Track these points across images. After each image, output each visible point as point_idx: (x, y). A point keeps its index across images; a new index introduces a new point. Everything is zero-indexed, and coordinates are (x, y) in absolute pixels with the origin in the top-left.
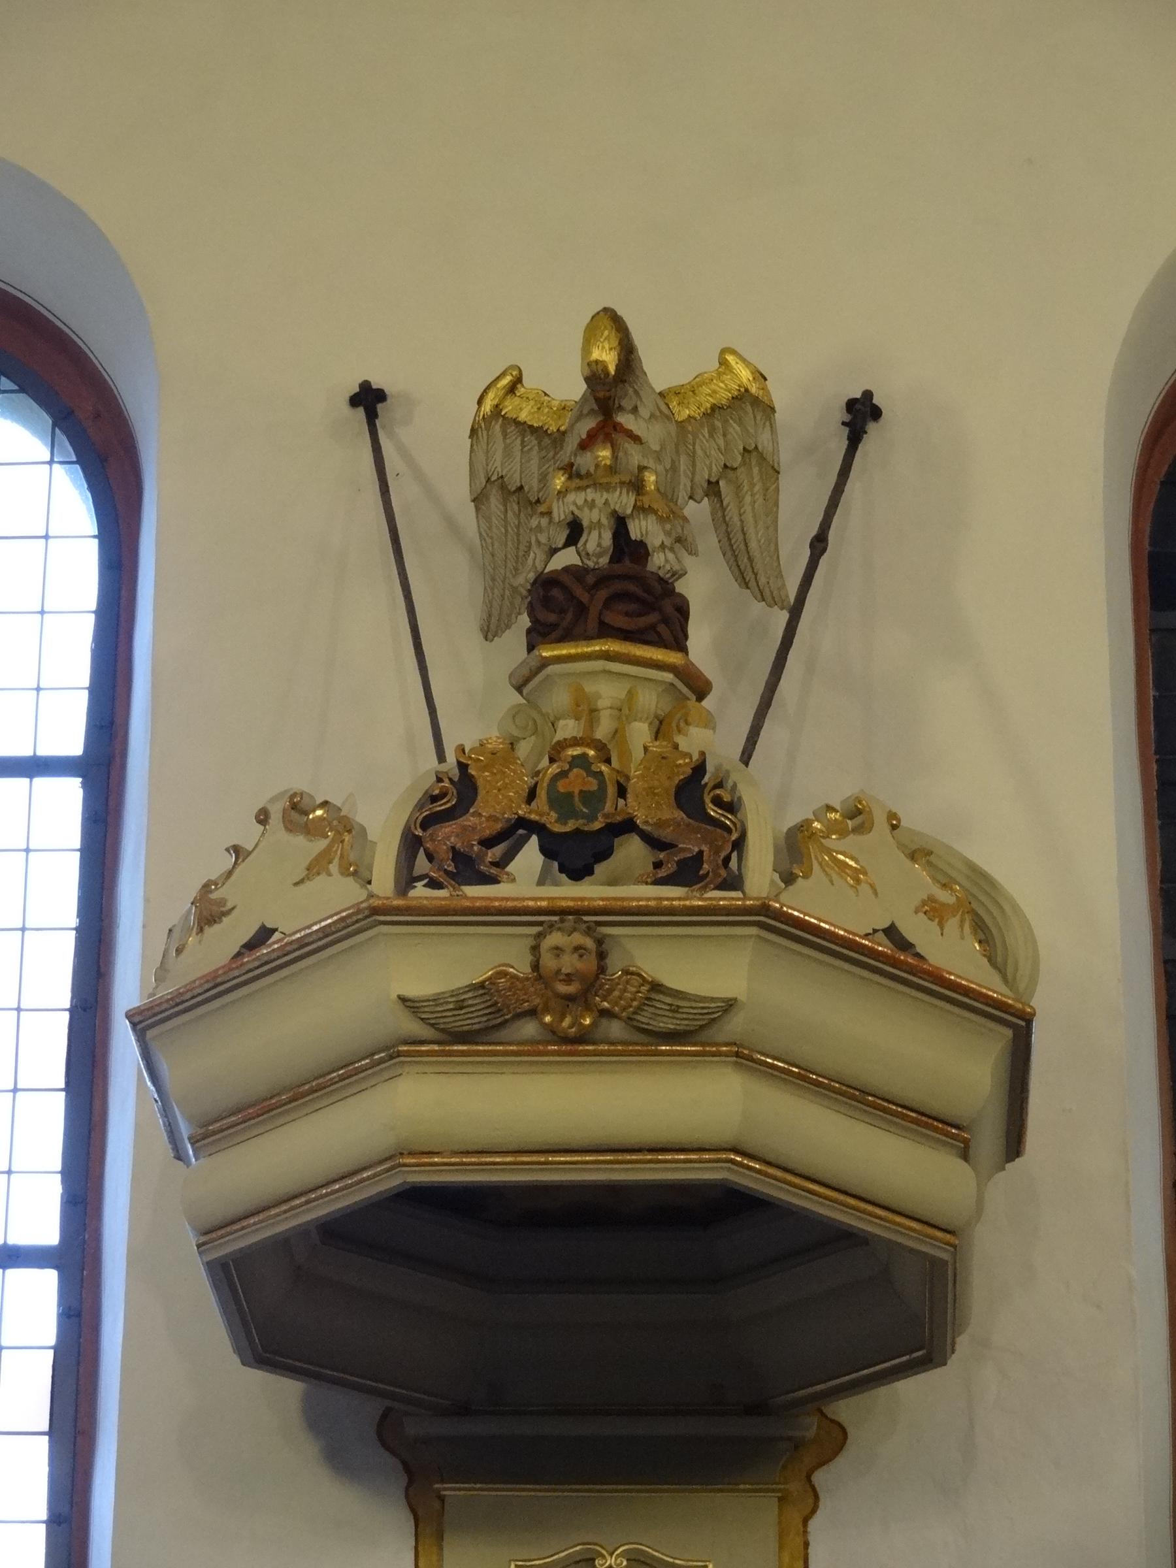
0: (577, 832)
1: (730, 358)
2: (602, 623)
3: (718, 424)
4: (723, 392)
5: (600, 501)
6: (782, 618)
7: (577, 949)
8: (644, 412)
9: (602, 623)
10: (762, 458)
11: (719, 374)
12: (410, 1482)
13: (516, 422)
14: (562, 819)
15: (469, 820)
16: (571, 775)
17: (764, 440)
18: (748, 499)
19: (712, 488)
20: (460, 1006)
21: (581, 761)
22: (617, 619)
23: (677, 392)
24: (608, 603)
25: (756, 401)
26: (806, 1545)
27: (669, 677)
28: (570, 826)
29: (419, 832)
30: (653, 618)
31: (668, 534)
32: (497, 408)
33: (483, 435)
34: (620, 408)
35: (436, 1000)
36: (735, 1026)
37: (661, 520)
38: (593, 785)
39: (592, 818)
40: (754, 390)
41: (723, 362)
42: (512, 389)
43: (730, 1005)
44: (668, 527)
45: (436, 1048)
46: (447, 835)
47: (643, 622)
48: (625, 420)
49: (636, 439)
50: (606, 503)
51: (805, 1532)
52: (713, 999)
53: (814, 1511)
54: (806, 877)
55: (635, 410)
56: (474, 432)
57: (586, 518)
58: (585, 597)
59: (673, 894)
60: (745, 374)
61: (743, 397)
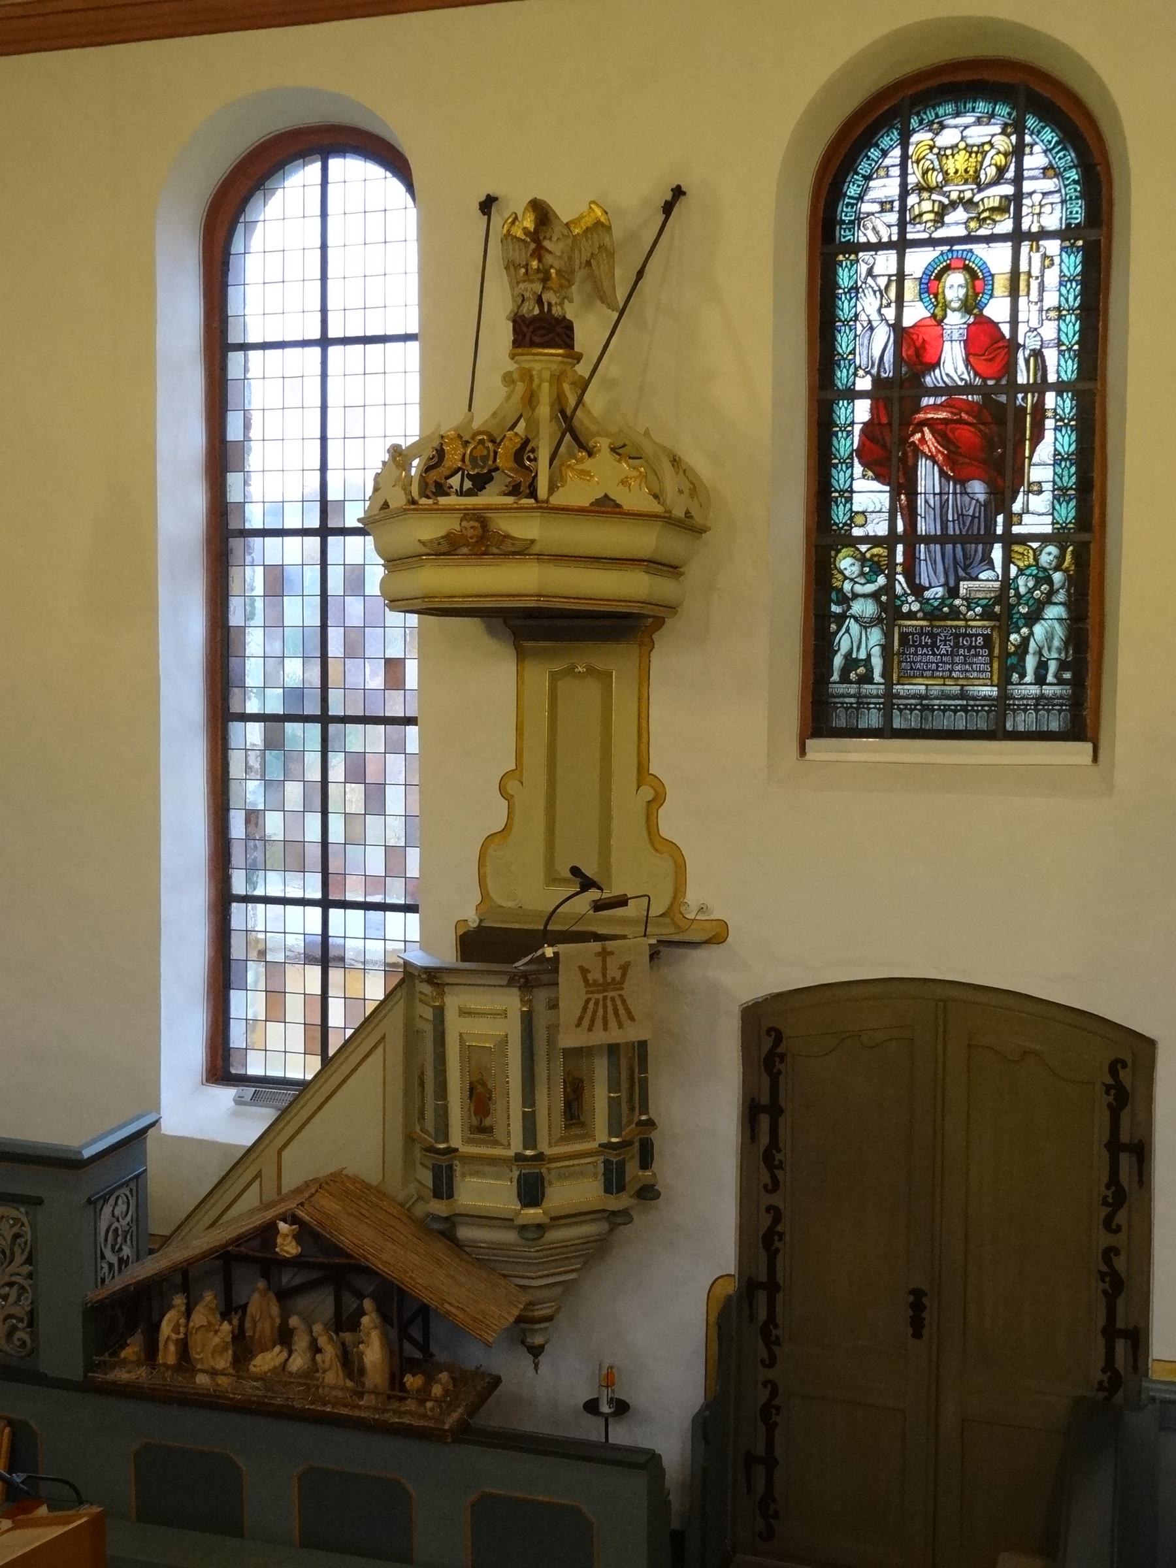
0: (478, 473)
1: (592, 206)
2: (531, 340)
3: (589, 236)
4: (589, 221)
5: (529, 290)
6: (616, 315)
7: (472, 527)
8: (554, 239)
9: (531, 340)
10: (606, 249)
11: (589, 213)
12: (515, 639)
13: (516, 237)
14: (473, 469)
15: (440, 469)
16: (478, 447)
17: (607, 241)
18: (602, 267)
19: (588, 263)
20: (439, 544)
21: (482, 442)
22: (537, 340)
23: (572, 222)
24: (533, 332)
25: (603, 225)
26: (650, 661)
27: (560, 359)
28: (476, 471)
29: (424, 475)
30: (551, 335)
31: (558, 298)
32: (509, 231)
33: (504, 242)
34: (545, 238)
35: (431, 541)
36: (536, 549)
37: (555, 292)
38: (485, 453)
39: (483, 468)
40: (602, 219)
41: (591, 208)
42: (513, 223)
43: (533, 542)
44: (558, 295)
45: (434, 557)
46: (433, 476)
47: (546, 338)
48: (546, 244)
49: (550, 252)
50: (532, 289)
51: (649, 657)
52: (526, 540)
53: (651, 650)
54: (563, 486)
55: (550, 239)
56: (502, 241)
57: (527, 295)
58: (525, 329)
59: (510, 500)
60: (599, 212)
61: (598, 223)
